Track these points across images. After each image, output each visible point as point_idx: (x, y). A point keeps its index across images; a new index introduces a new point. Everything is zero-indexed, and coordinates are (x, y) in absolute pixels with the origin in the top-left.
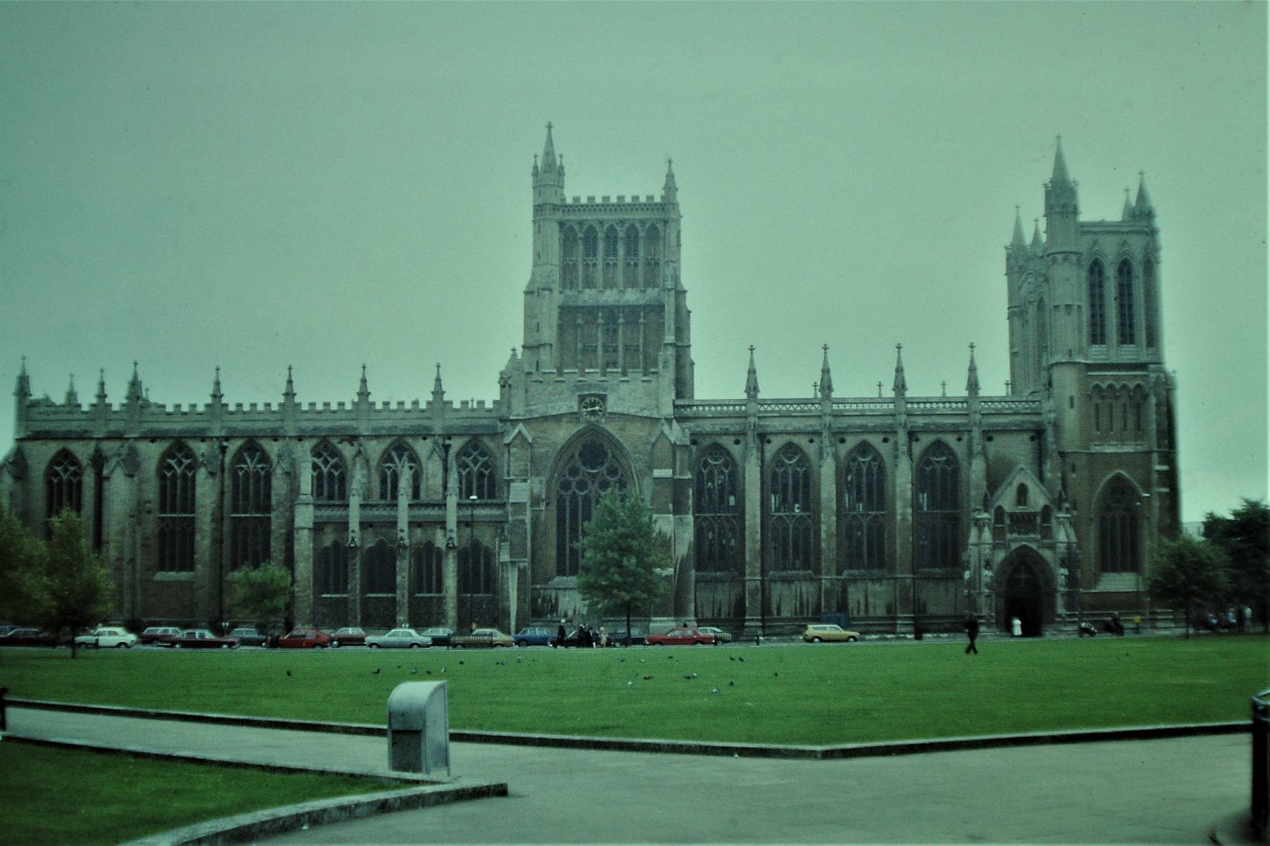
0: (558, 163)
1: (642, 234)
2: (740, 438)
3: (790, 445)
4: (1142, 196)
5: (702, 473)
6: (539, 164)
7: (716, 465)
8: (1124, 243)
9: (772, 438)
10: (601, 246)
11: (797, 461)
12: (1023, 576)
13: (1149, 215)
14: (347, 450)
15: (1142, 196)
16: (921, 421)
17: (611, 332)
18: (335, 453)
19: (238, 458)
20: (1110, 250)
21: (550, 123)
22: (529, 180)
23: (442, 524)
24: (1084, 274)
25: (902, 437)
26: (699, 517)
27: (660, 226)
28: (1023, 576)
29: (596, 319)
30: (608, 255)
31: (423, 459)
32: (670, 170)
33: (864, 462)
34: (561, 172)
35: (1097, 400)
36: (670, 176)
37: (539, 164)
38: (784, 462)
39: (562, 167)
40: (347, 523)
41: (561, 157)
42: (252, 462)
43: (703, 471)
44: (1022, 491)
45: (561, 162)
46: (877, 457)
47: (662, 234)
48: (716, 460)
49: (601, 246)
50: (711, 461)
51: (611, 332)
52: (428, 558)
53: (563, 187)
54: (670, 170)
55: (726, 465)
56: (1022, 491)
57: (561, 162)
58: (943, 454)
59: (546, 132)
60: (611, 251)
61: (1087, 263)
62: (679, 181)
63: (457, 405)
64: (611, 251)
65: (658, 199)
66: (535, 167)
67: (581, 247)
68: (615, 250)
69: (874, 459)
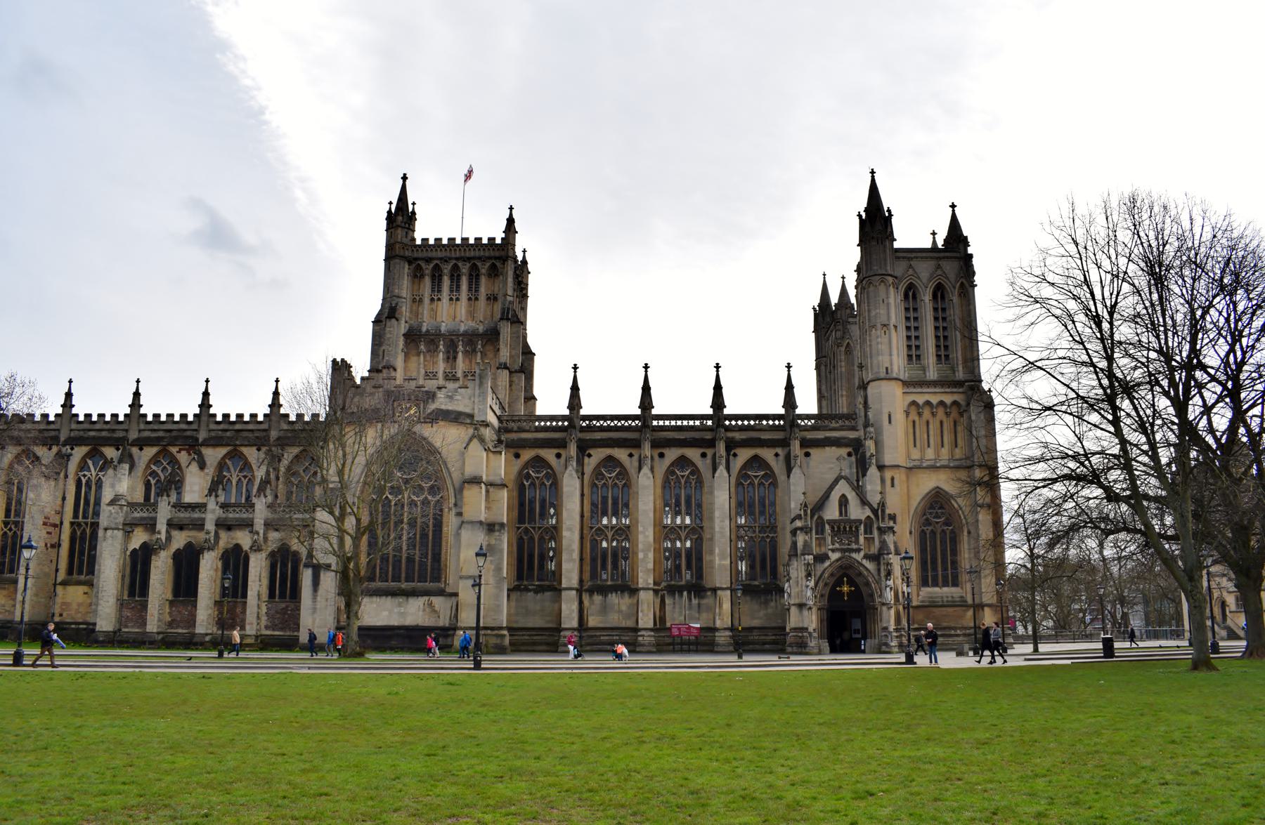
0: (410, 210)
1: (483, 271)
2: (561, 451)
3: (610, 458)
4: (954, 224)
5: (524, 485)
6: (393, 210)
7: (538, 478)
8: (939, 267)
9: (592, 451)
10: (446, 282)
11: (617, 474)
12: (845, 589)
13: (964, 242)
14: (183, 457)
15: (954, 224)
16: (738, 436)
17: (451, 358)
18: (174, 462)
19: (83, 466)
20: (924, 270)
21: (405, 175)
22: (384, 224)
23: (248, 525)
24: (900, 296)
25: (721, 448)
26: (518, 528)
27: (498, 264)
28: (845, 589)
29: (438, 347)
30: (451, 291)
31: (254, 467)
32: (511, 214)
33: (683, 476)
34: (412, 217)
35: (913, 415)
36: (511, 221)
37: (393, 210)
38: (603, 475)
39: (414, 213)
40: (155, 524)
41: (414, 204)
42: (95, 470)
43: (525, 483)
44: (843, 501)
45: (413, 209)
46: (696, 471)
47: (500, 270)
48: (538, 472)
49: (446, 282)
50: (533, 474)
51: (451, 358)
52: (235, 562)
53: (414, 231)
54: (511, 214)
55: (547, 476)
56: (843, 501)
57: (413, 209)
58: (759, 469)
59: (401, 182)
60: (455, 287)
61: (902, 287)
62: (517, 226)
63: (293, 418)
64: (455, 287)
65: (498, 241)
66: (389, 212)
67: (427, 281)
68: (458, 287)
69: (692, 473)
